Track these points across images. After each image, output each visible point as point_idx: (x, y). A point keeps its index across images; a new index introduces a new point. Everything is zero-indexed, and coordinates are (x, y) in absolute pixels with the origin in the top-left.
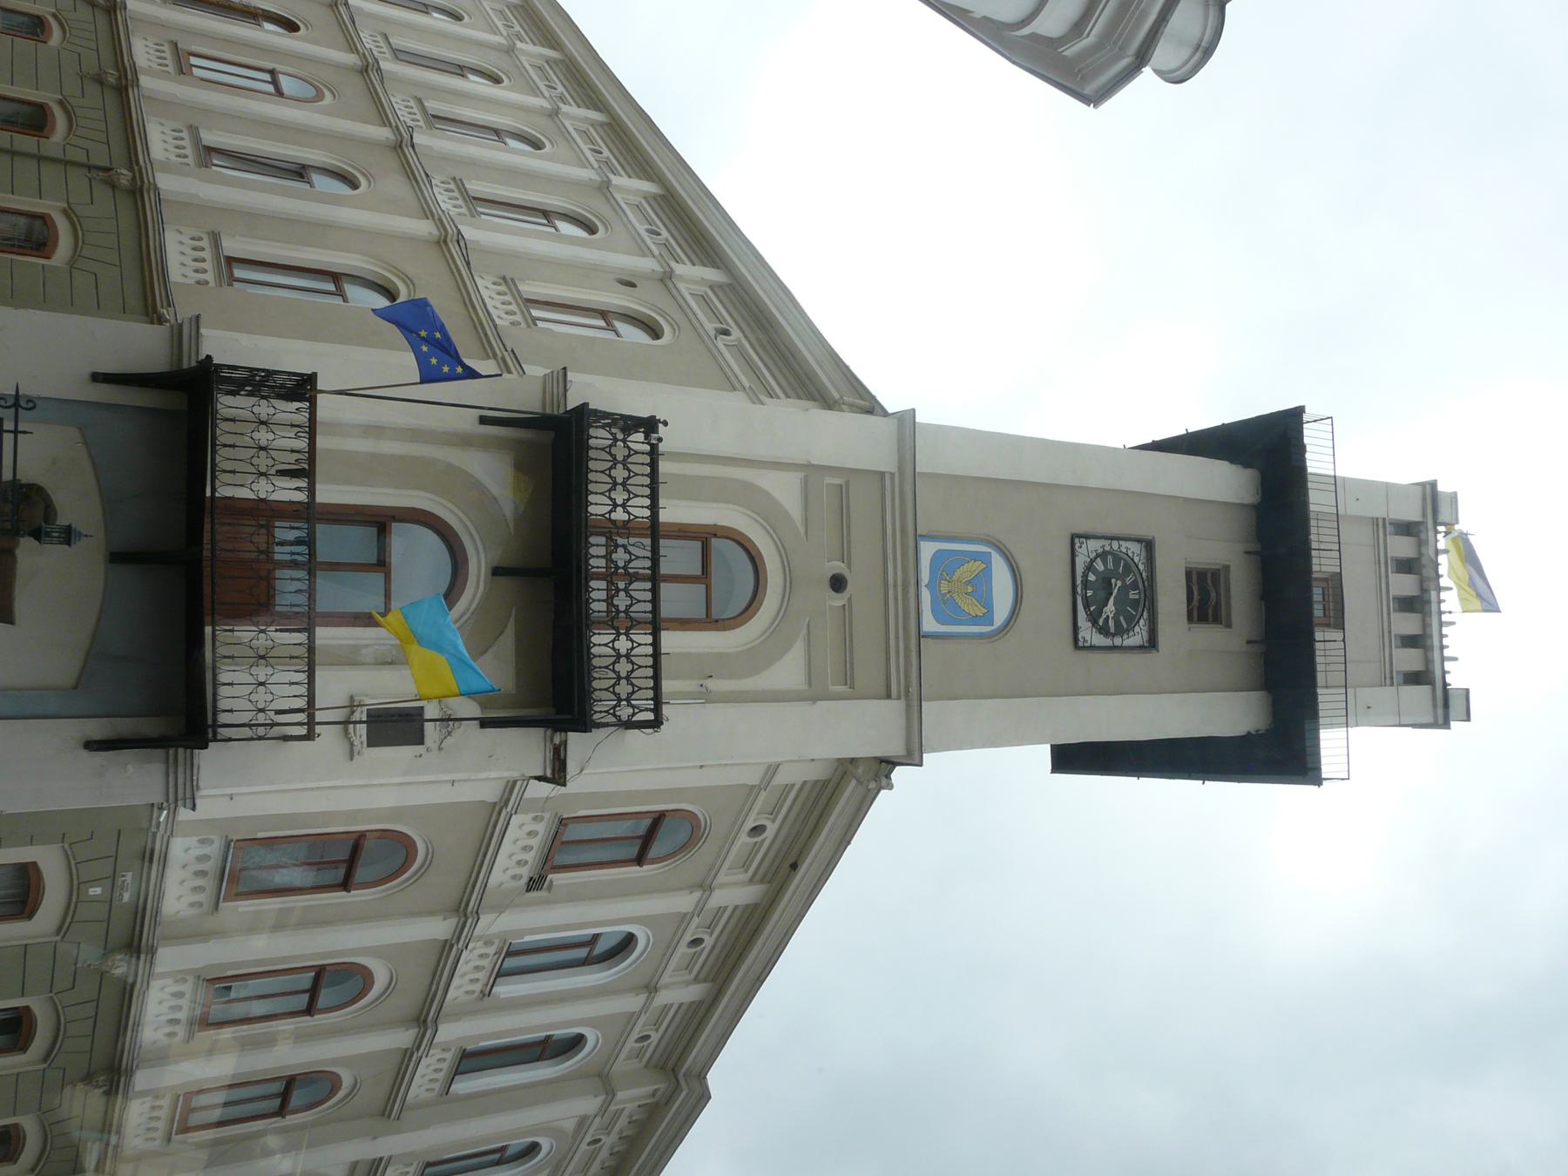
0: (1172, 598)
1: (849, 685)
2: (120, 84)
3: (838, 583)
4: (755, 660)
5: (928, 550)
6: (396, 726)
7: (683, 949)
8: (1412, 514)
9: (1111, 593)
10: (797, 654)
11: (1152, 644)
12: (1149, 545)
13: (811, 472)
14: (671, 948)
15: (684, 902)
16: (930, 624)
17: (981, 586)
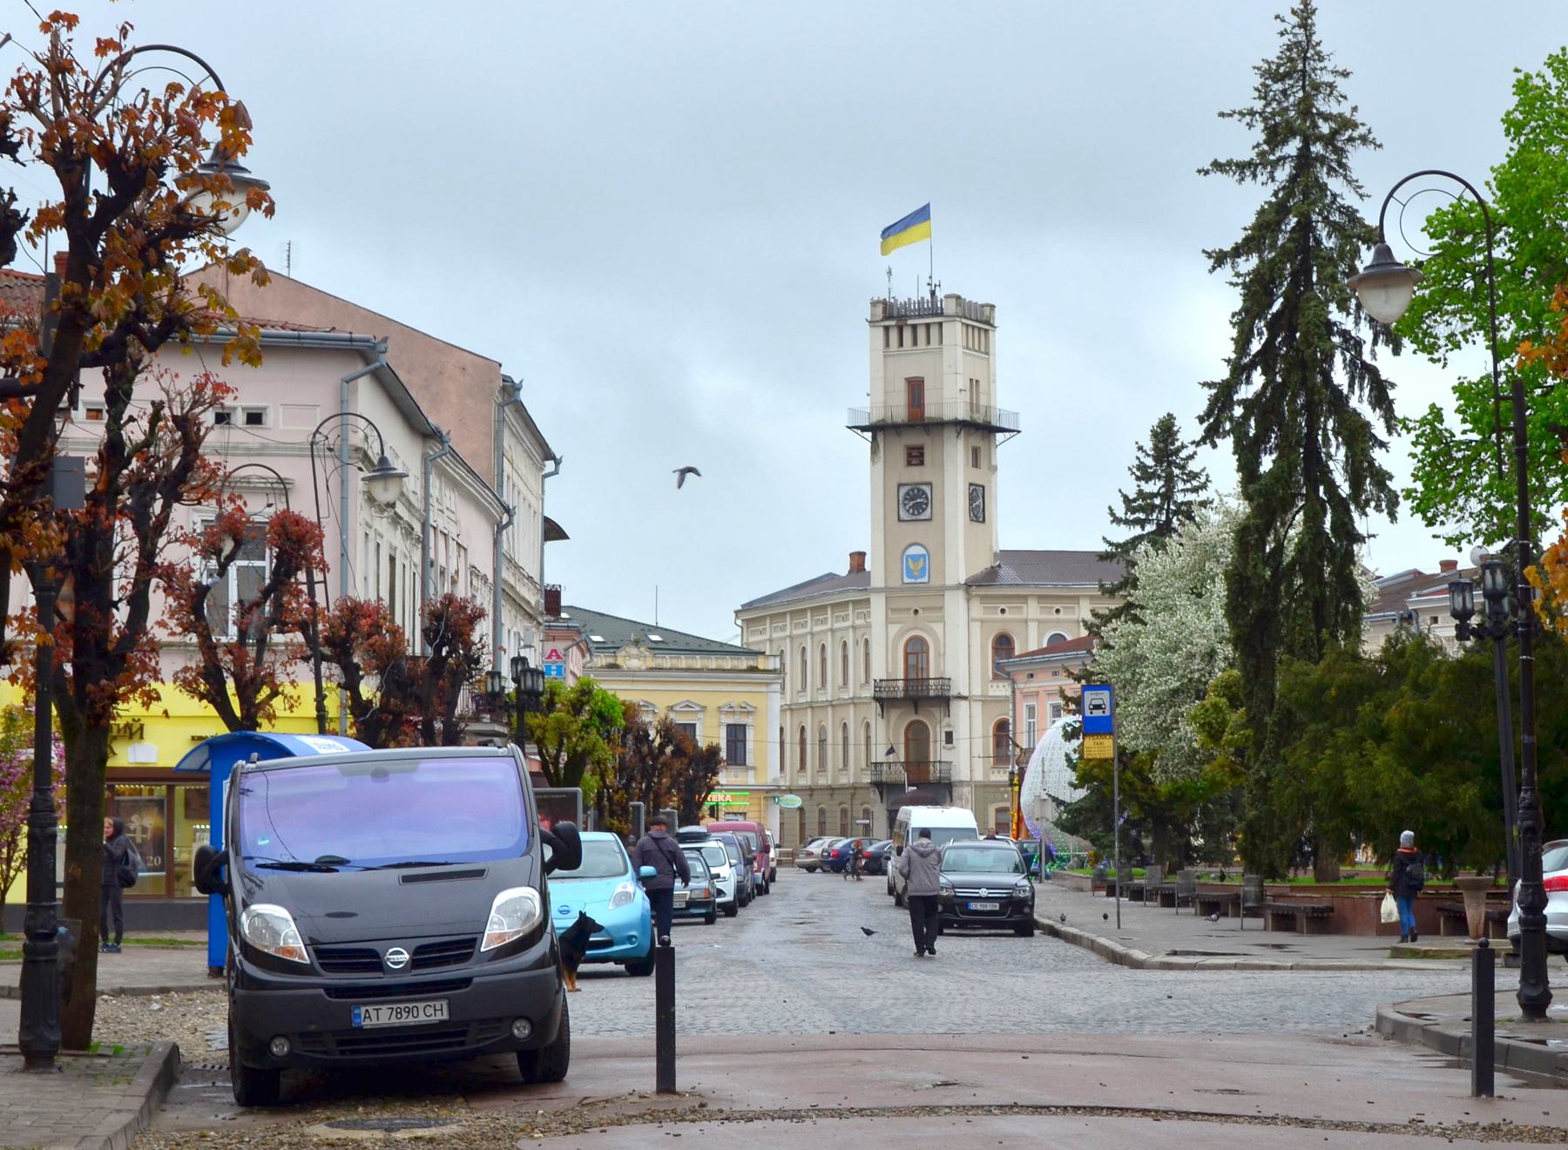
0: (915, 474)
1: (941, 608)
2: (832, 790)
3: (916, 612)
4: (936, 640)
5: (906, 580)
6: (949, 737)
7: (1061, 616)
8: (880, 332)
9: (915, 502)
10: (934, 625)
11: (930, 484)
12: (900, 485)
13: (888, 621)
14: (1058, 621)
15: (1033, 627)
16: (925, 579)
17: (916, 558)
